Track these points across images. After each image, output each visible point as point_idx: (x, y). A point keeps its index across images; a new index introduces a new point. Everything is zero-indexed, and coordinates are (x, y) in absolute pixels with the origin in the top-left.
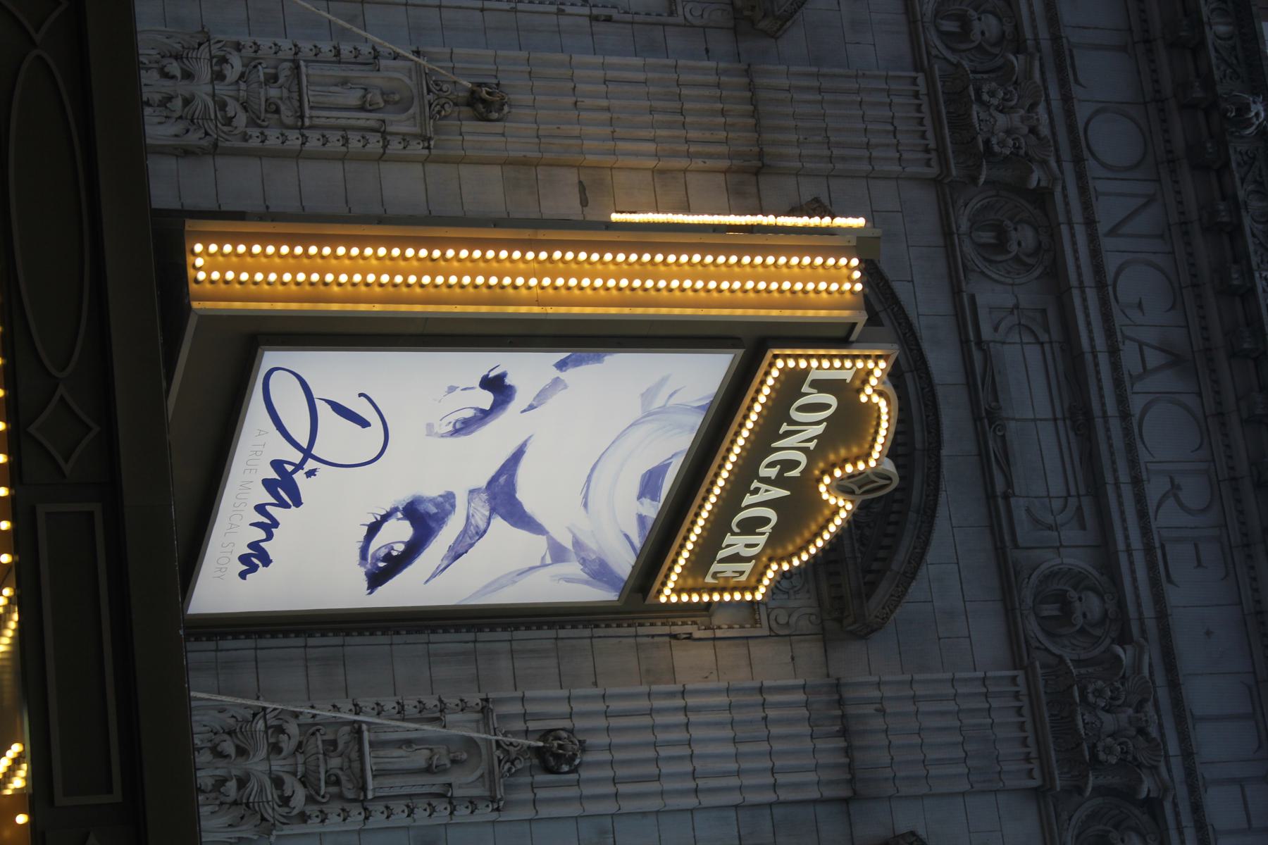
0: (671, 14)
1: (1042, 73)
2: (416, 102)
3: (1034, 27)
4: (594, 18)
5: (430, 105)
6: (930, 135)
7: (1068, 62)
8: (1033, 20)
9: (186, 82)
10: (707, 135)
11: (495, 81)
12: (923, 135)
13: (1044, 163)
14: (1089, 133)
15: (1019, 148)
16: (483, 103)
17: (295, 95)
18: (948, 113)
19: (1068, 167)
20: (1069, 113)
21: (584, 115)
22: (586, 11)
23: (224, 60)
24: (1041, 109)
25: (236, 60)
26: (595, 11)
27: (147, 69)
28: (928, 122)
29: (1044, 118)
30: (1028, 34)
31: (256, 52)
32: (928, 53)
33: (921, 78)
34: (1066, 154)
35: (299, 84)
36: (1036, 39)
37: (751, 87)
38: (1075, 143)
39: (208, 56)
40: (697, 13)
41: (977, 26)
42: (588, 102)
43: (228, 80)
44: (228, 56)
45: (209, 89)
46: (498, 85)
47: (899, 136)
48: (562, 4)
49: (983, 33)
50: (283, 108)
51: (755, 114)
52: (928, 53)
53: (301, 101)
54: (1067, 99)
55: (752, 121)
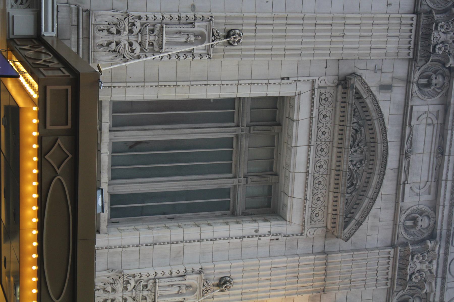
0: (302, 234)
1: (439, 249)
2: (198, 290)
3: (442, 225)
4: (273, 240)
5: (203, 291)
6: (390, 273)
7: (451, 240)
8: (442, 222)
9: (113, 293)
10: (305, 285)
11: (229, 275)
12: (387, 274)
13: (430, 283)
14: (451, 265)
15: (423, 277)
16: (223, 283)
17: (153, 294)
18: (399, 264)
19: (439, 280)
20: (445, 260)
21: (261, 284)
22: (269, 238)
23: (128, 282)
24: (435, 262)
25: (132, 282)
26: (273, 238)
27: (98, 290)
28: (390, 268)
29: (435, 267)
30: (439, 228)
31: (140, 277)
32: (398, 236)
33: (392, 251)
34: (440, 275)
35: (155, 289)
36: (441, 230)
37: (326, 264)
38: (444, 272)
39: (122, 282)
40: (312, 233)
41: (420, 223)
42: (263, 278)
43: (128, 291)
44: (130, 281)
45: (121, 295)
46: (229, 277)
47: (378, 274)
48: (260, 236)
49: (421, 226)
50: (148, 298)
51: (325, 275)
52: (398, 236)
53: (155, 296)
54: (446, 254)
55: (324, 277)
